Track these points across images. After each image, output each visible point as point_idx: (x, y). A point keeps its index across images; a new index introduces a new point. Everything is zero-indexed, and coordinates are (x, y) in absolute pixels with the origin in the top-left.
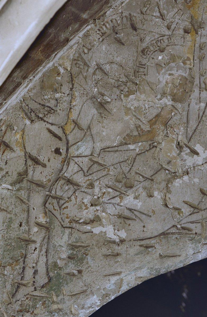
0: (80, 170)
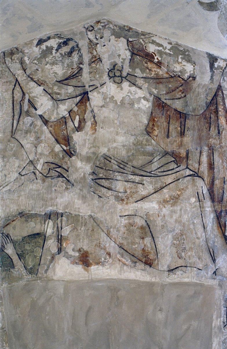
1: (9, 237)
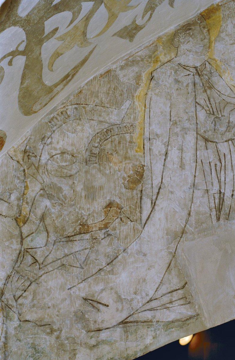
0: (35, 262)
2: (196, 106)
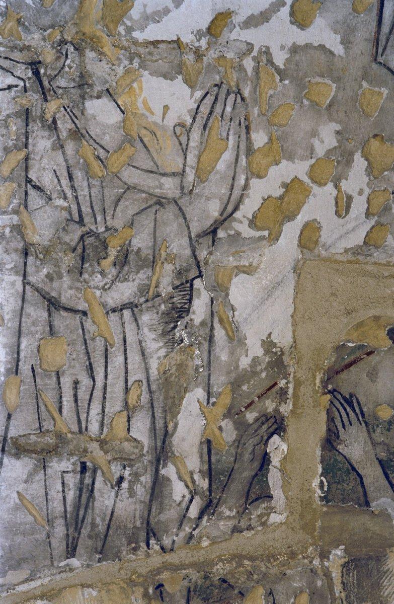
1: (355, 404)
2: (26, 193)
